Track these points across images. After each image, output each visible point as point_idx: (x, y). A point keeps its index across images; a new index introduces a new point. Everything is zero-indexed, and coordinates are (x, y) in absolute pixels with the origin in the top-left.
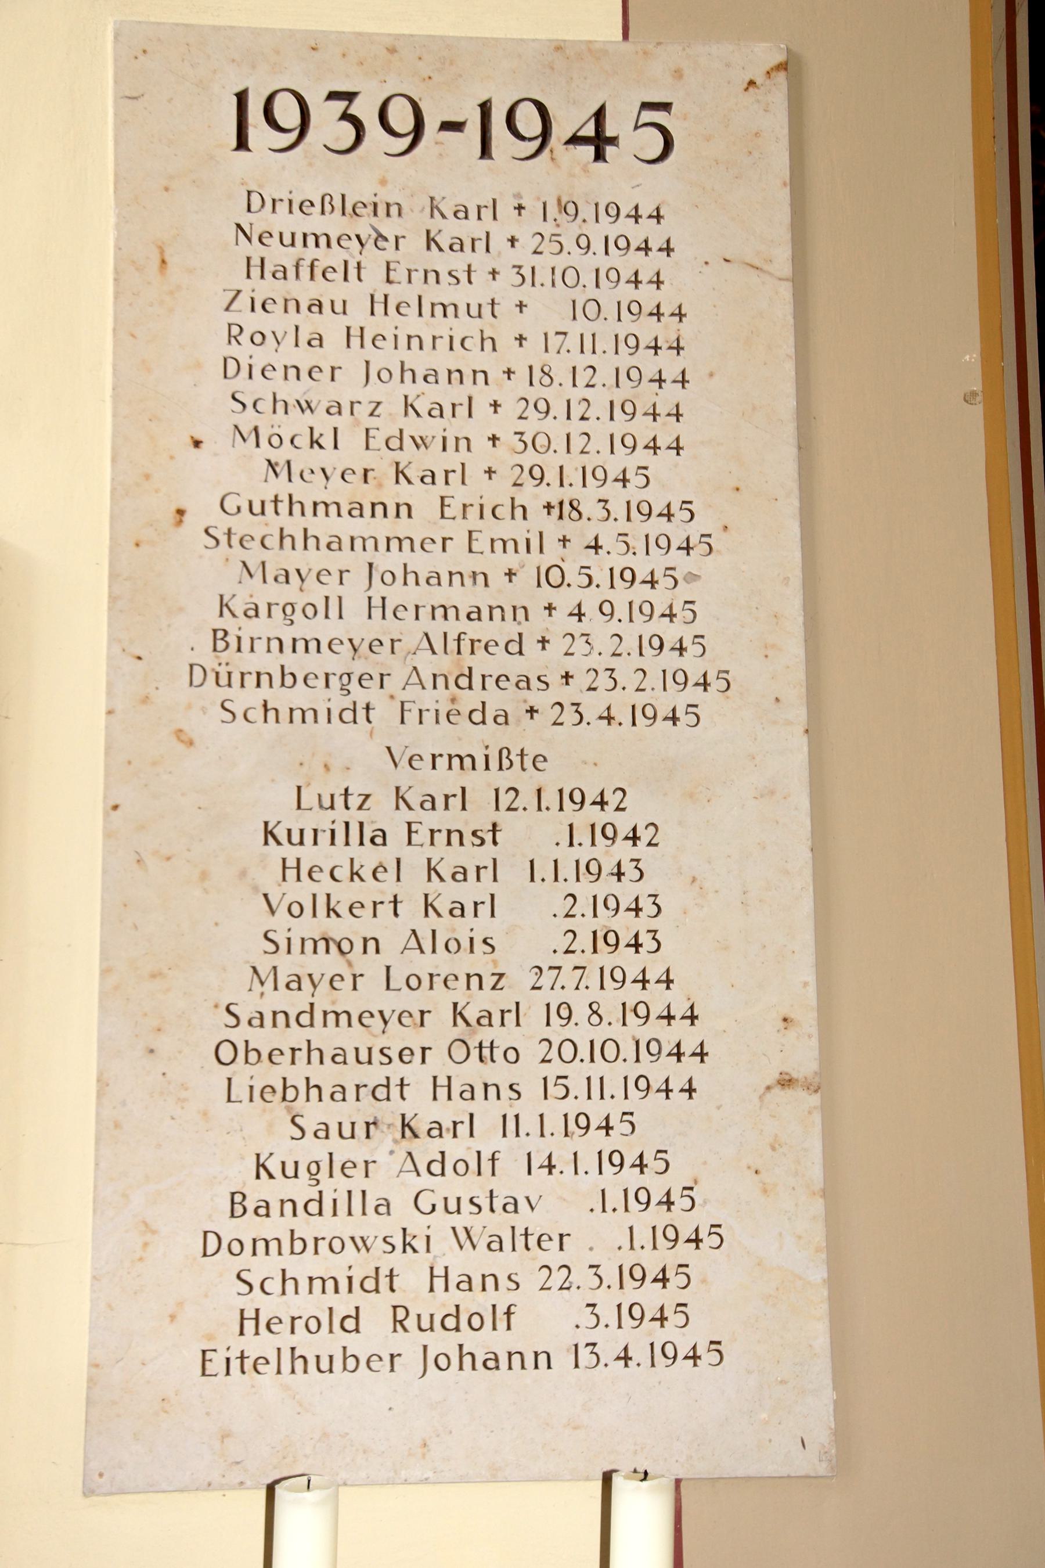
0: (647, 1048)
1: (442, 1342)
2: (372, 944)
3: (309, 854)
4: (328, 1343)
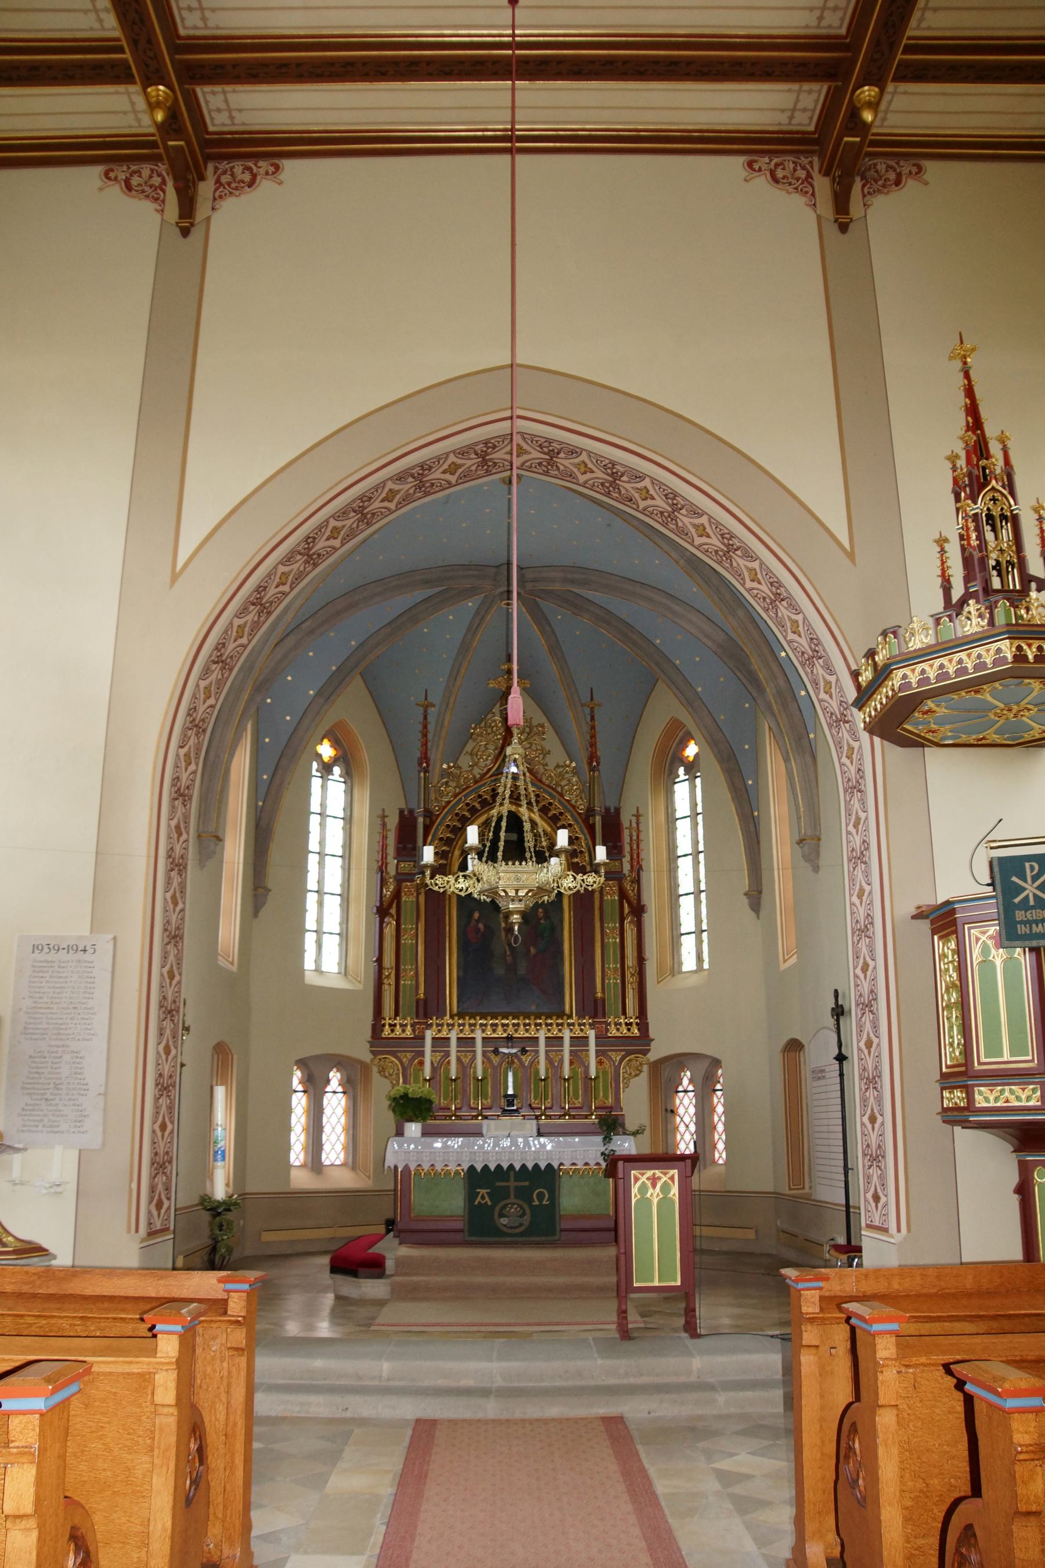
0: (80, 1089)
1: (49, 1129)
2: (43, 1073)
3: (36, 1060)
4: (34, 1129)
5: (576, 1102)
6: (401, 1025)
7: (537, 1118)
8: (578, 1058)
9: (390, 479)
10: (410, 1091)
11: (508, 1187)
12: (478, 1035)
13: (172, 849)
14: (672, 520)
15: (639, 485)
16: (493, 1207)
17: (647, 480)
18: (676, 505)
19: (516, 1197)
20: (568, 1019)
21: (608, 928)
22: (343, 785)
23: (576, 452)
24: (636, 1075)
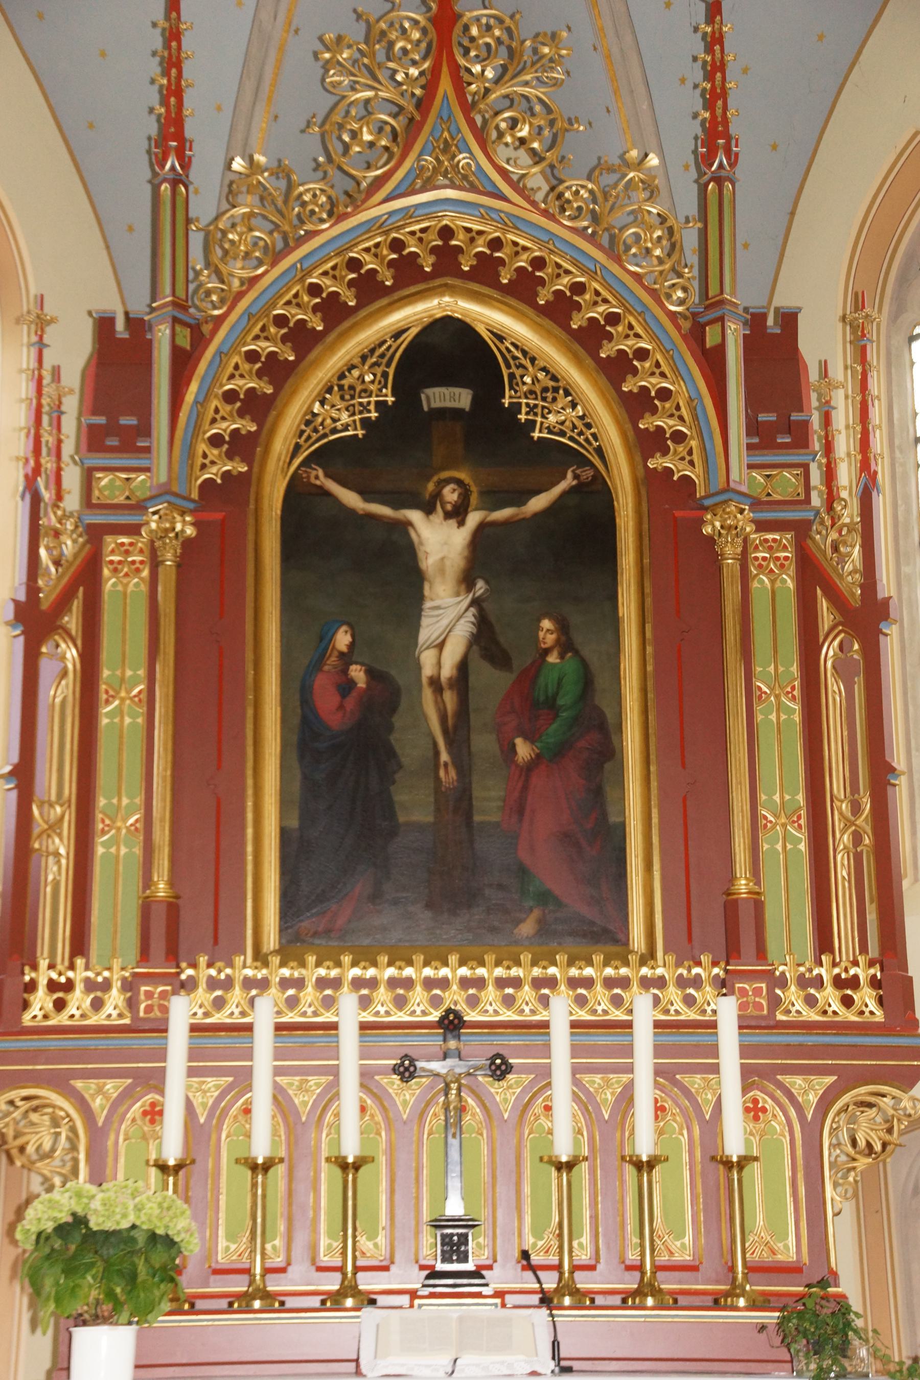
6: (90, 986)
7: (546, 1300)
20: (643, 962)
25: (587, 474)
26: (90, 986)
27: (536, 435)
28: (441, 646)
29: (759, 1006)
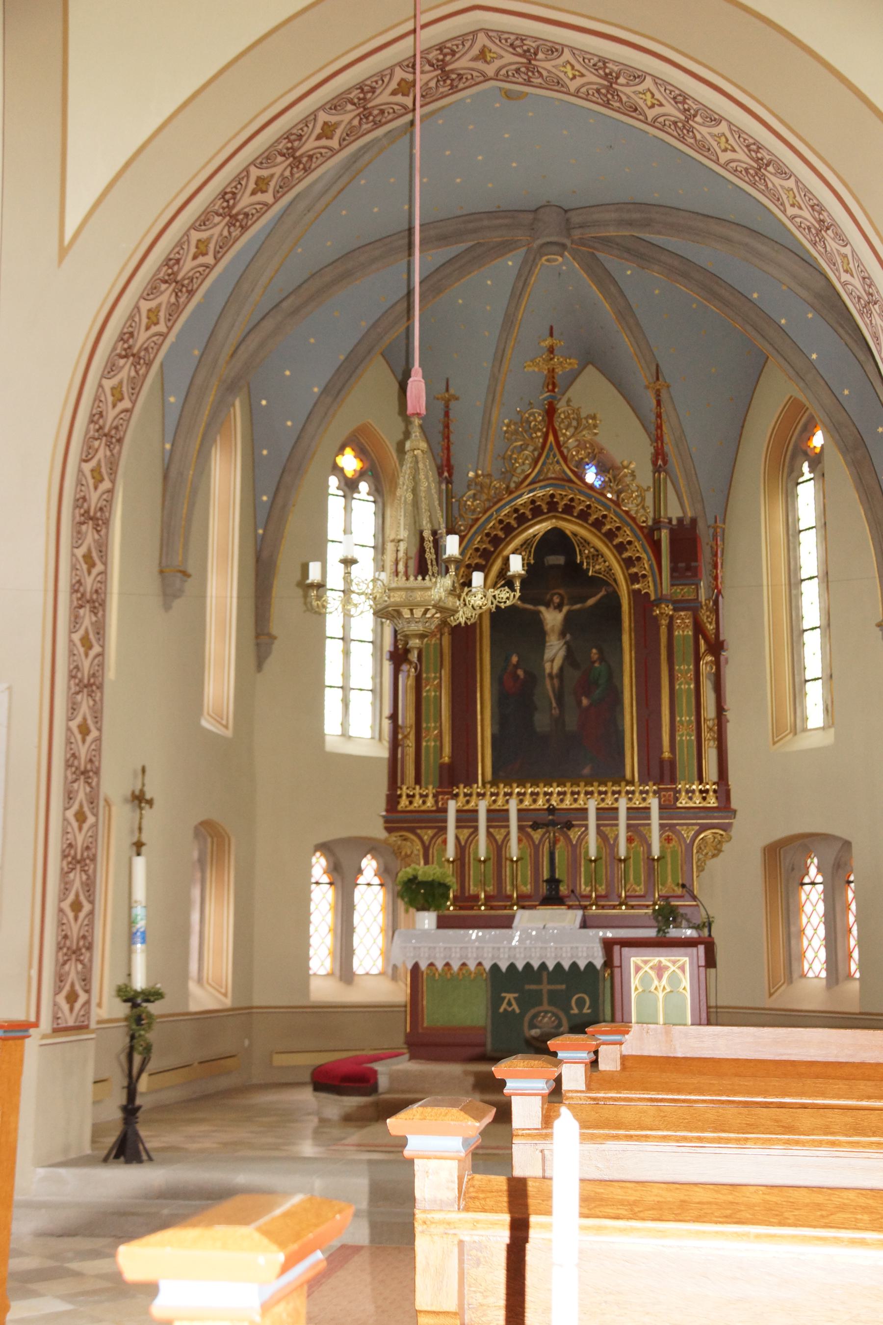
5: (638, 888)
6: (421, 796)
7: (585, 908)
8: (637, 834)
9: (322, 108)
10: (420, 873)
11: (541, 990)
12: (513, 807)
13: (79, 582)
14: (688, 131)
15: (640, 88)
16: (522, 1015)
17: (649, 79)
18: (689, 110)
19: (551, 1002)
21: (680, 671)
22: (373, 504)
23: (557, 50)
24: (714, 856)
25: (610, 590)
26: (421, 796)
27: (590, 574)
28: (552, 661)
29: (670, 801)
